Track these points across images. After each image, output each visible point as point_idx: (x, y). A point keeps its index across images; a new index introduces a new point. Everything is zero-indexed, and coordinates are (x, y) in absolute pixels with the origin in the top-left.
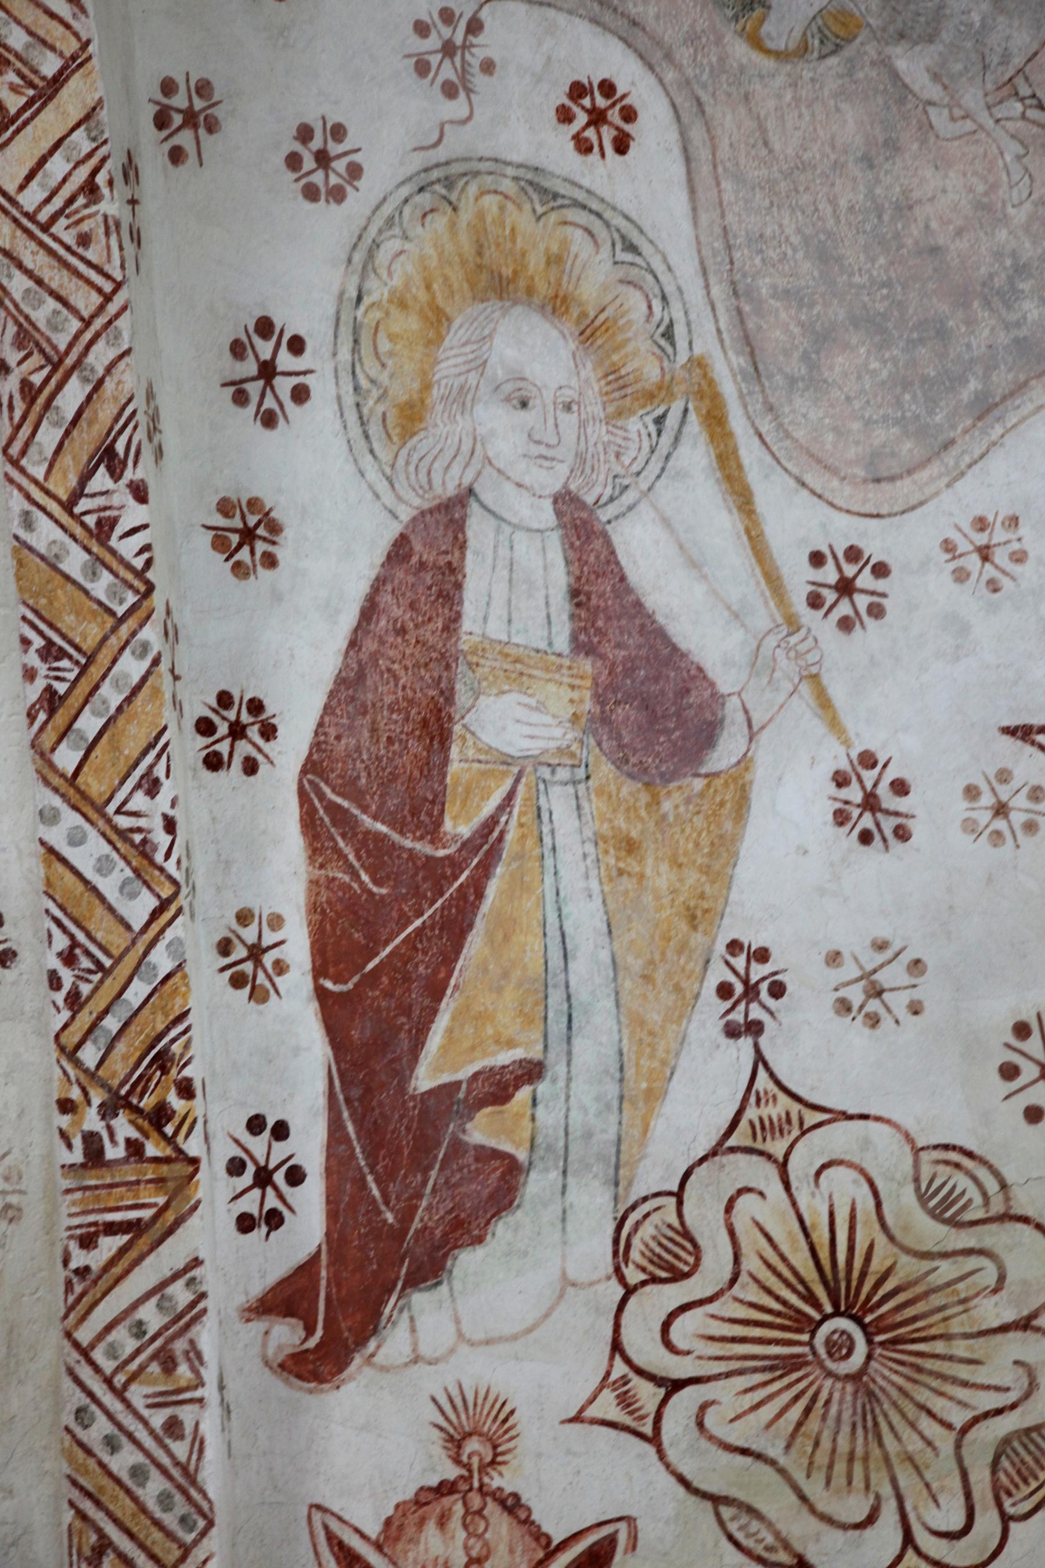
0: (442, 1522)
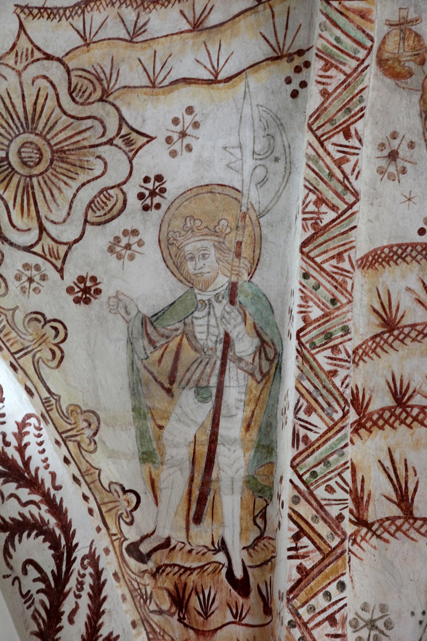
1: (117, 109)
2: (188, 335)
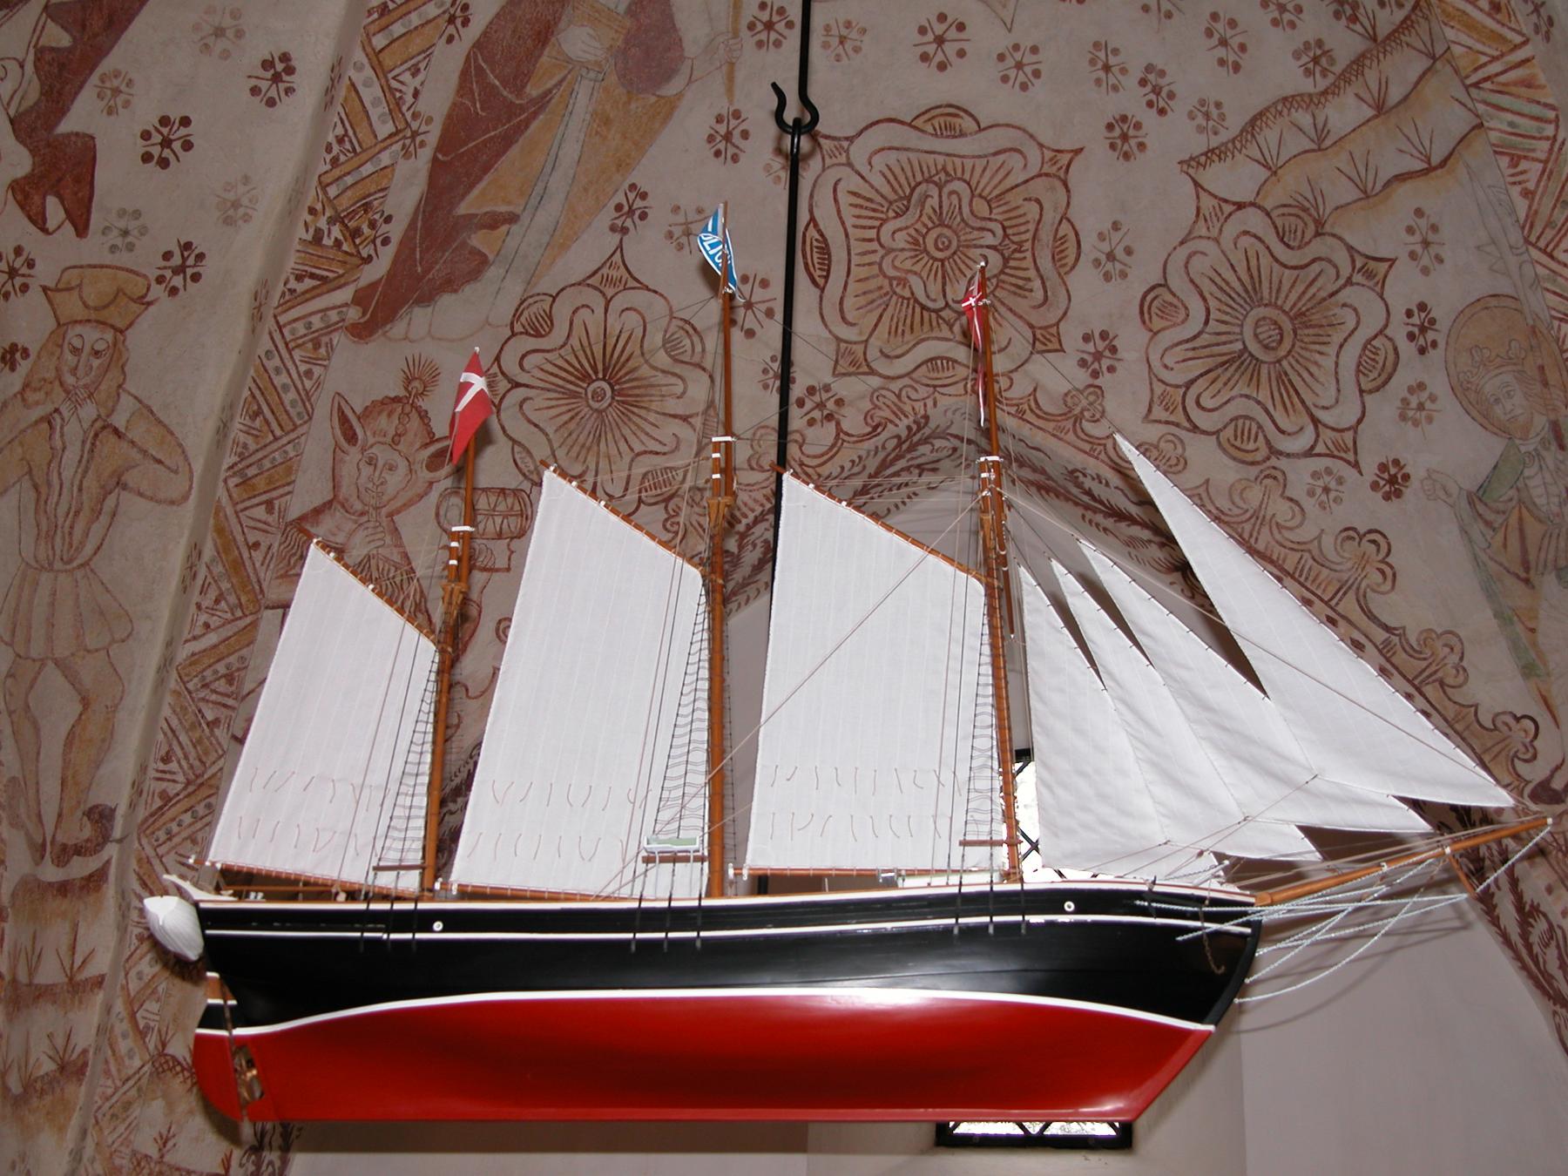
0: (389, 415)
1: (1340, 238)
2: (1525, 504)
